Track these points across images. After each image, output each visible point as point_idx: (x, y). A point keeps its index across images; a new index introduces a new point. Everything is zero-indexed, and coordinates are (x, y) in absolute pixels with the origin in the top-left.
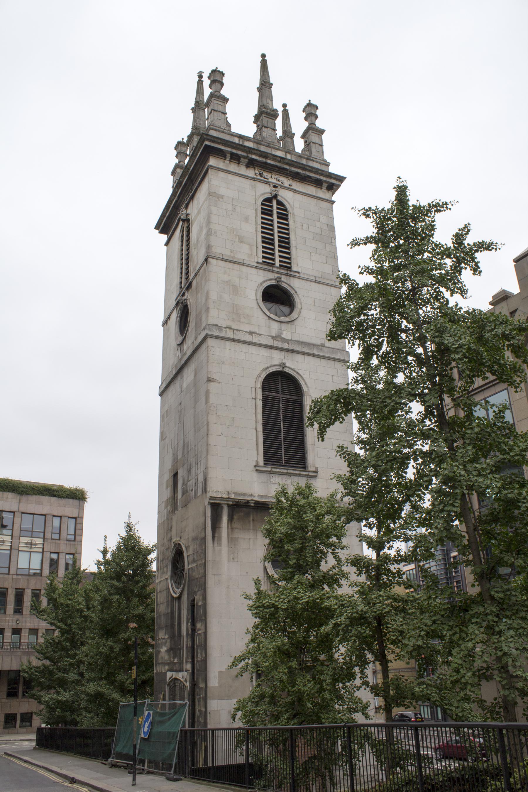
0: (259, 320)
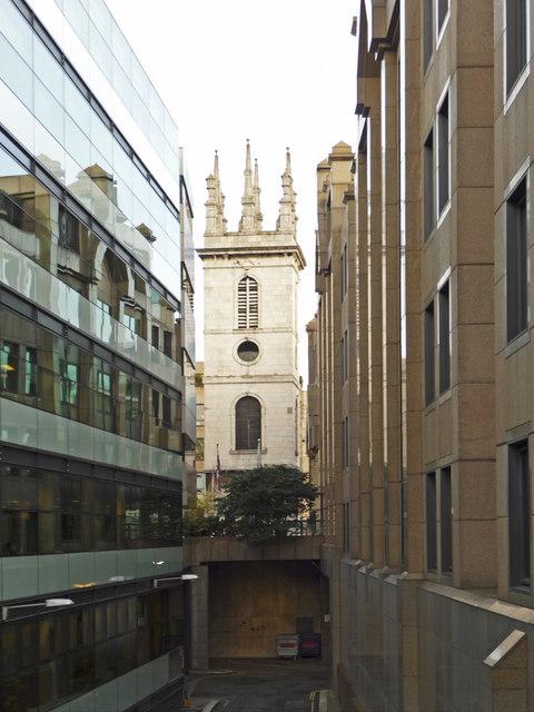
0: (236, 366)
